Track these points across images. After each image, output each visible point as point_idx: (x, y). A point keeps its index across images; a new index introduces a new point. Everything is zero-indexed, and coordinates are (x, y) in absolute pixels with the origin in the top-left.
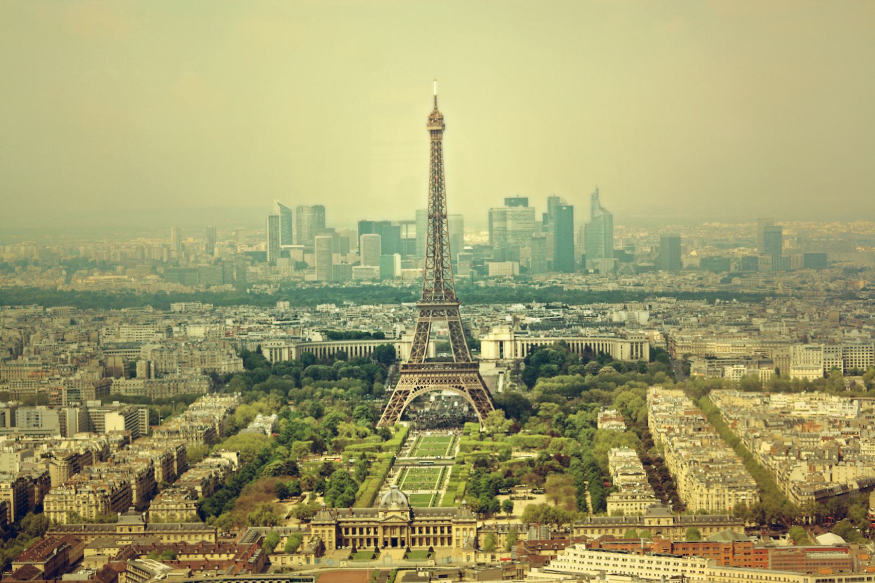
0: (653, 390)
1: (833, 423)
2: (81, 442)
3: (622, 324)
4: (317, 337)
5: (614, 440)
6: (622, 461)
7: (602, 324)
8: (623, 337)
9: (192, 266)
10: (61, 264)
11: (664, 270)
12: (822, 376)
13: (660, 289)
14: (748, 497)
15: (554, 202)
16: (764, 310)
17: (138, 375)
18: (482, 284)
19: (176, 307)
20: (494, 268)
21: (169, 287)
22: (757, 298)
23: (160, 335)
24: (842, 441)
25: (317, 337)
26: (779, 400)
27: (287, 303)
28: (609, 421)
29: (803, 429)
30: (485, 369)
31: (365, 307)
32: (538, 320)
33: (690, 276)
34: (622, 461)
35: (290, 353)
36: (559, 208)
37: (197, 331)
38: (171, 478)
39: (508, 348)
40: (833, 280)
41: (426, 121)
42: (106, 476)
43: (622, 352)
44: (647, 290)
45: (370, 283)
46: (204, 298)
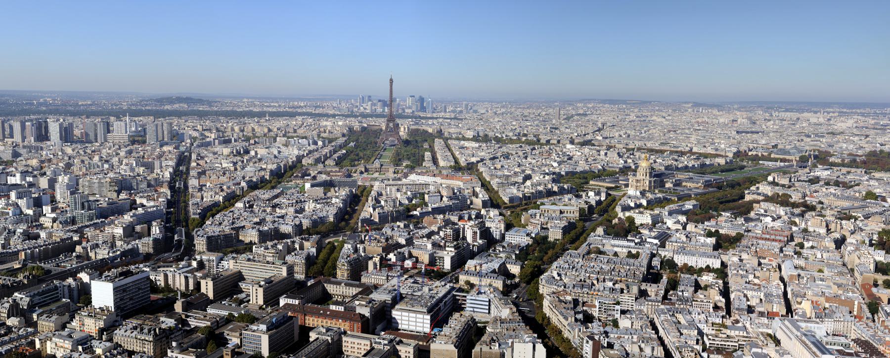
1: (473, 148)
2: (313, 147)
5: (426, 150)
6: (428, 155)
14: (453, 164)
21: (336, 113)
22: (461, 119)
26: (462, 142)
28: (426, 145)
30: (401, 133)
34: (428, 155)
37: (340, 123)
38: (331, 156)
42: (317, 155)
43: (430, 130)
46: (343, 115)
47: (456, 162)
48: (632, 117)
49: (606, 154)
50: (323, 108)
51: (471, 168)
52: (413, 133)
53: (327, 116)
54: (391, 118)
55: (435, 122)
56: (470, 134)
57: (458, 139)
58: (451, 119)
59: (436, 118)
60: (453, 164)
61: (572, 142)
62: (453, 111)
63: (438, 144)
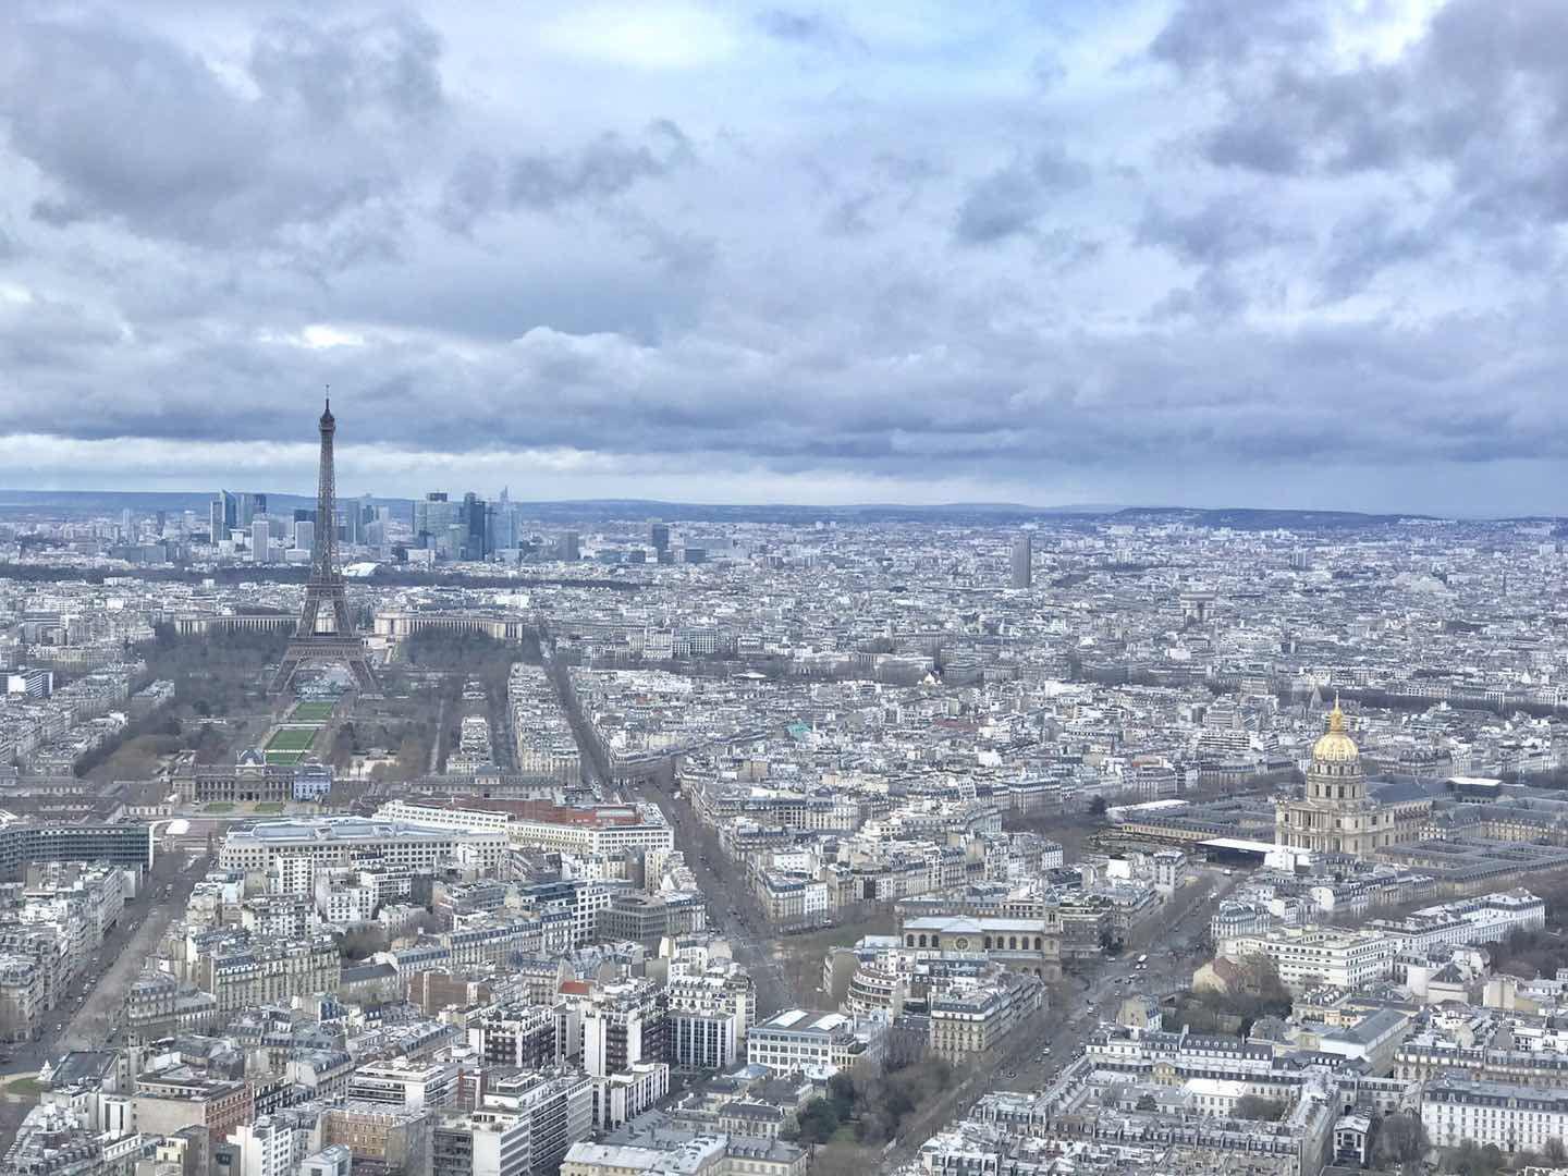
0: (516, 666)
1: (663, 696)
3: (503, 607)
4: (227, 612)
7: (483, 606)
8: (501, 618)
9: (139, 545)
10: (17, 539)
11: (562, 559)
12: (670, 656)
13: (552, 577)
15: (471, 498)
16: (632, 599)
17: (55, 641)
18: (399, 568)
19: (109, 581)
20: (412, 554)
22: (632, 588)
23: (82, 607)
24: (669, 713)
25: (227, 612)
26: (623, 676)
27: (212, 581)
29: (638, 703)
31: (282, 586)
32: (429, 601)
33: (585, 566)
34: (474, 726)
35: (200, 626)
36: (473, 503)
39: (398, 624)
40: (706, 573)
41: (319, 422)
43: (498, 631)
44: (544, 578)
45: (300, 565)
47: (591, 748)
48: (1321, 574)
49: (1199, 716)
50: (57, 543)
51: (657, 779)
53: (70, 574)
55: (522, 600)
56: (661, 646)
57: (609, 663)
58: (589, 584)
59: (533, 583)
60: (575, 760)
61: (1074, 669)
62: (605, 557)
63: (525, 678)
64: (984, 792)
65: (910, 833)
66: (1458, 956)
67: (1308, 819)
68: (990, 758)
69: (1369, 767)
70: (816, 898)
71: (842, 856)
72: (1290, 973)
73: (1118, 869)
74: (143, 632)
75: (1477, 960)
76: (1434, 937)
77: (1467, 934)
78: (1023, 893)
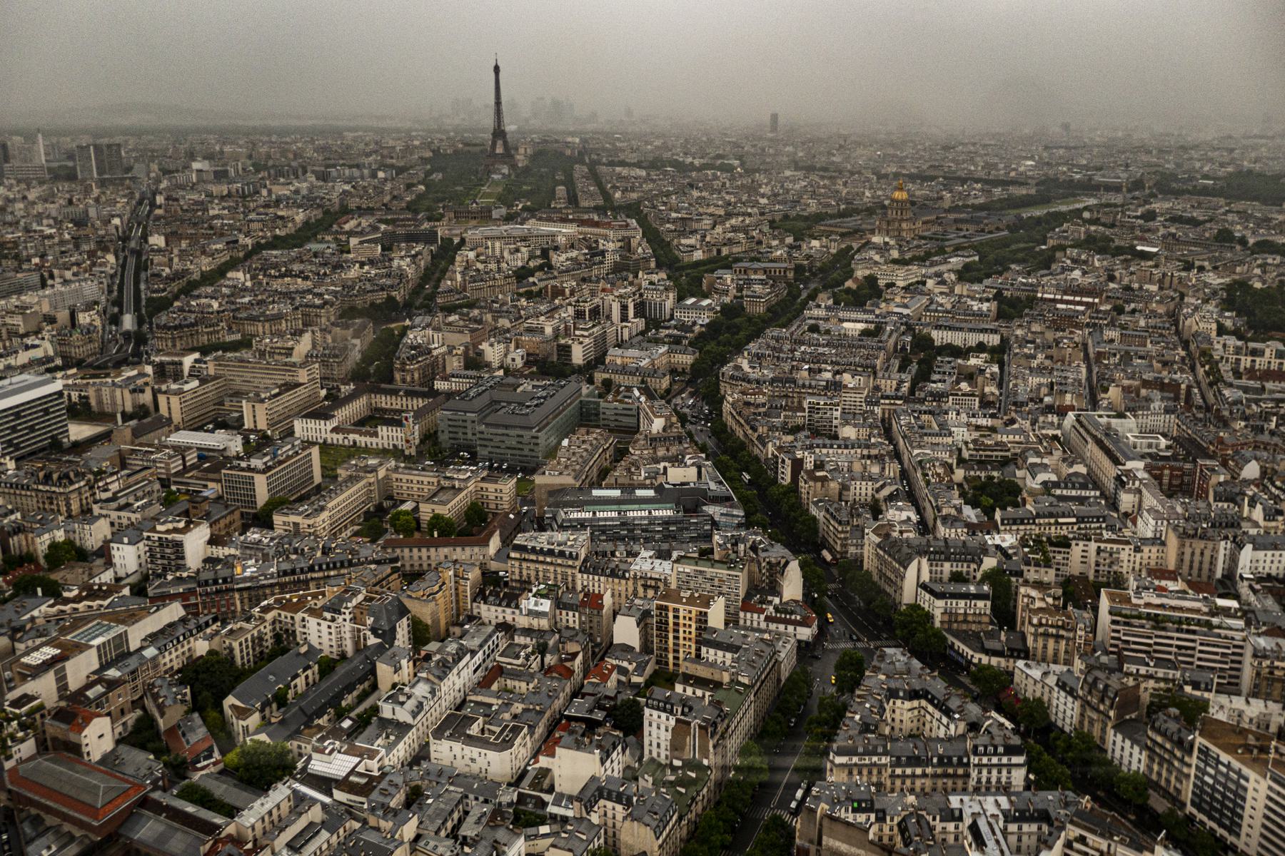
6: (561, 190)
26: (618, 169)
34: (561, 190)
51: (632, 209)
52: (538, 155)
54: (499, 133)
63: (580, 170)
64: (762, 214)
65: (734, 229)
66: (946, 275)
67: (888, 223)
68: (764, 201)
69: (913, 203)
70: (698, 255)
71: (708, 239)
72: (882, 283)
73: (815, 243)
74: (429, 154)
75: (953, 277)
76: (936, 269)
77: (949, 266)
78: (779, 253)
